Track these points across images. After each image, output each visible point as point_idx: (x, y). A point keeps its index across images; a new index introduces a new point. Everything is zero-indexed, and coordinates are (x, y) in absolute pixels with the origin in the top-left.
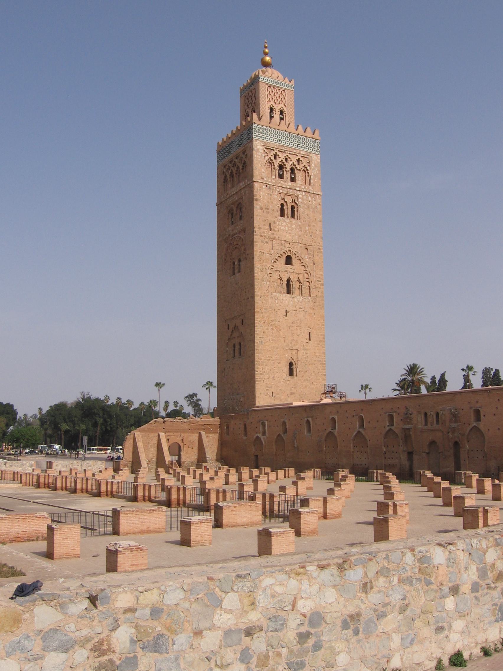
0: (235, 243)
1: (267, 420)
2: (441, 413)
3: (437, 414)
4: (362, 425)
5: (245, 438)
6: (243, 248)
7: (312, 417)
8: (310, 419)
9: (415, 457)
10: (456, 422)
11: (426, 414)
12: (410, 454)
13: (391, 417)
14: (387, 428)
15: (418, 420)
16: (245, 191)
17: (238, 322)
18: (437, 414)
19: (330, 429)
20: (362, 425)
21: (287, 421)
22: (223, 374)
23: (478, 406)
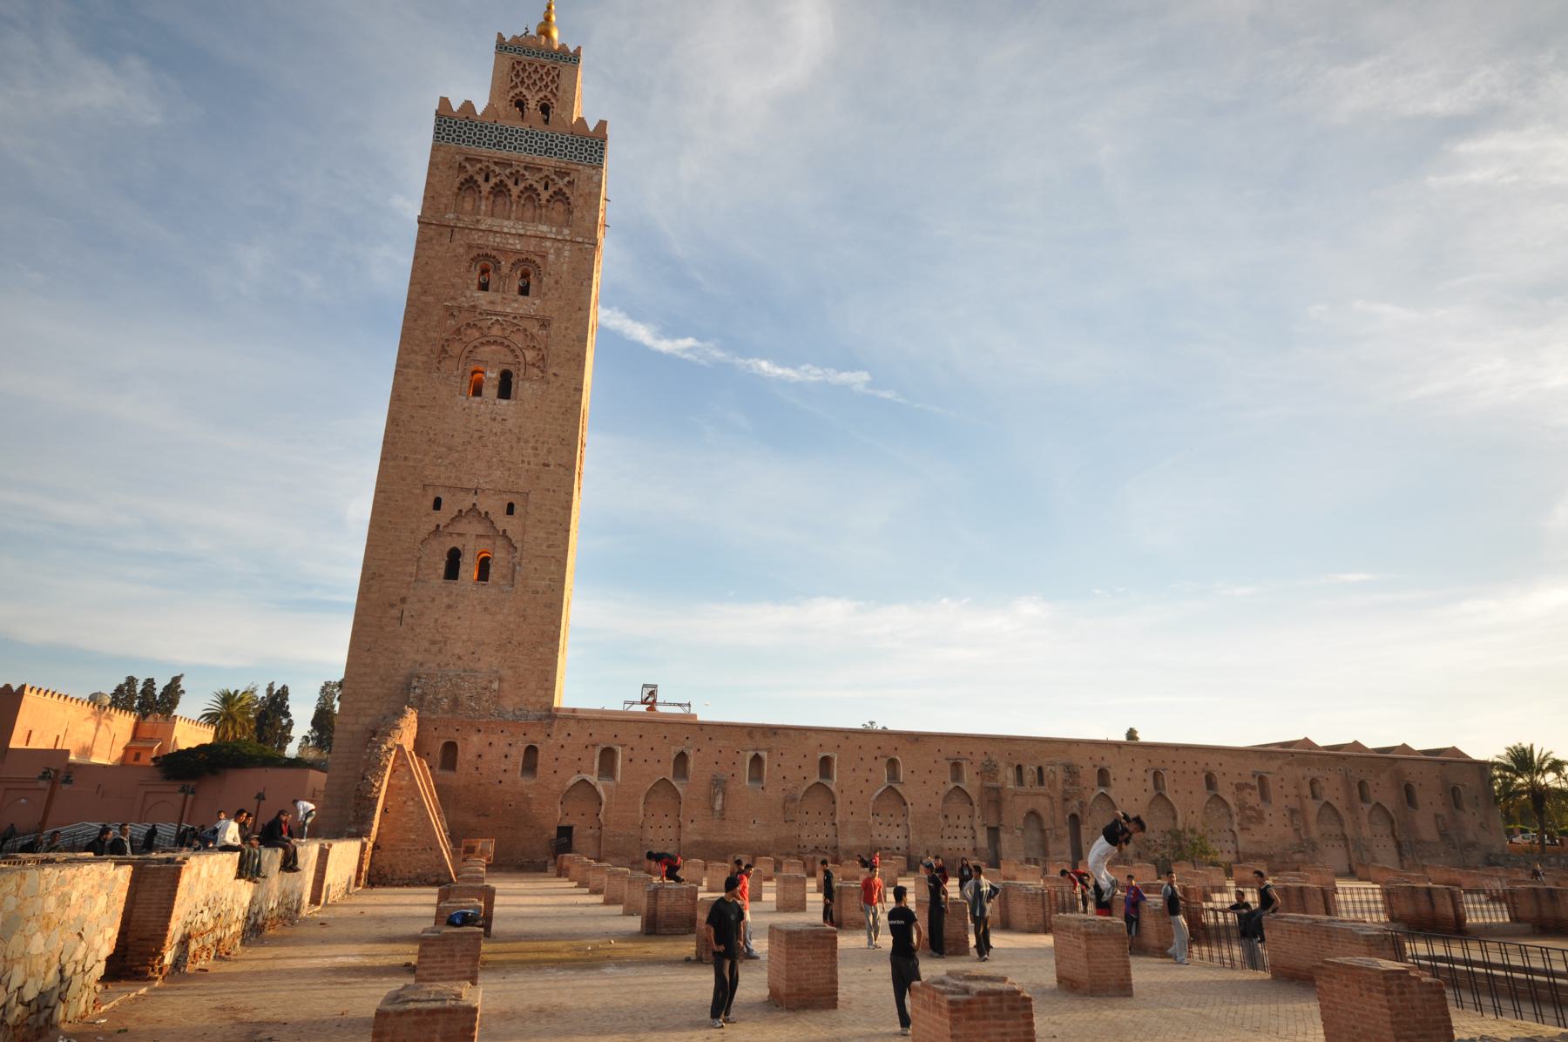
0: (496, 331)
1: (623, 746)
2: (1047, 770)
3: (1040, 769)
4: (893, 776)
5: (525, 782)
6: (530, 355)
7: (769, 751)
8: (764, 754)
9: (1004, 836)
10: (1072, 784)
11: (1019, 768)
12: (994, 832)
13: (956, 766)
14: (951, 786)
15: (1007, 776)
16: (559, 253)
17: (492, 504)
18: (1040, 769)
19: (817, 779)
20: (893, 776)
21: (691, 753)
22: (395, 612)
23: (1104, 764)
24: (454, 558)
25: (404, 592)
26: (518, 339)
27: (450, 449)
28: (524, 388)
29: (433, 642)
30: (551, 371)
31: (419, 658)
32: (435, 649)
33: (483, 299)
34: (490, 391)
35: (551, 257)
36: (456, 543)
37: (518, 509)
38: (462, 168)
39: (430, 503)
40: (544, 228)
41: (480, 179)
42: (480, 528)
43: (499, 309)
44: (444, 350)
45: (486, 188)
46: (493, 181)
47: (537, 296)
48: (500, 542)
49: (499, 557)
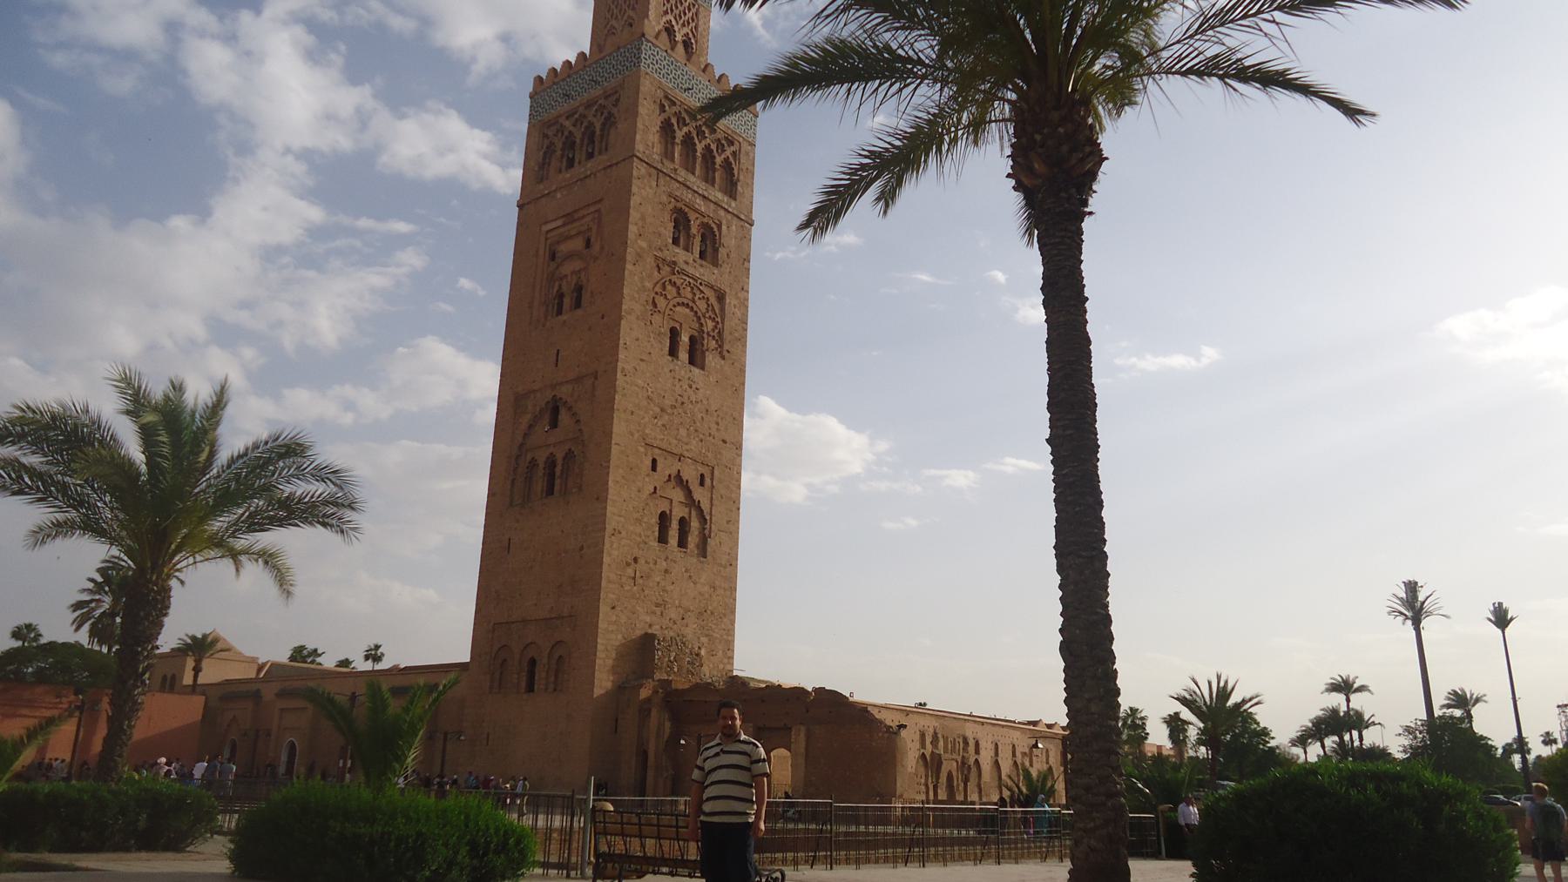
17: (690, 474)
24: (664, 518)
25: (637, 552)
26: (702, 305)
27: (662, 410)
28: (711, 359)
29: (657, 605)
30: (726, 347)
31: (648, 619)
32: (658, 610)
33: (680, 255)
34: (684, 355)
35: (724, 227)
36: (664, 506)
37: (708, 481)
38: (662, 107)
39: (649, 463)
40: (720, 195)
41: (674, 121)
42: (678, 495)
43: (690, 270)
44: (655, 305)
45: (679, 135)
46: (685, 129)
47: (715, 263)
48: (694, 513)
49: (695, 524)
